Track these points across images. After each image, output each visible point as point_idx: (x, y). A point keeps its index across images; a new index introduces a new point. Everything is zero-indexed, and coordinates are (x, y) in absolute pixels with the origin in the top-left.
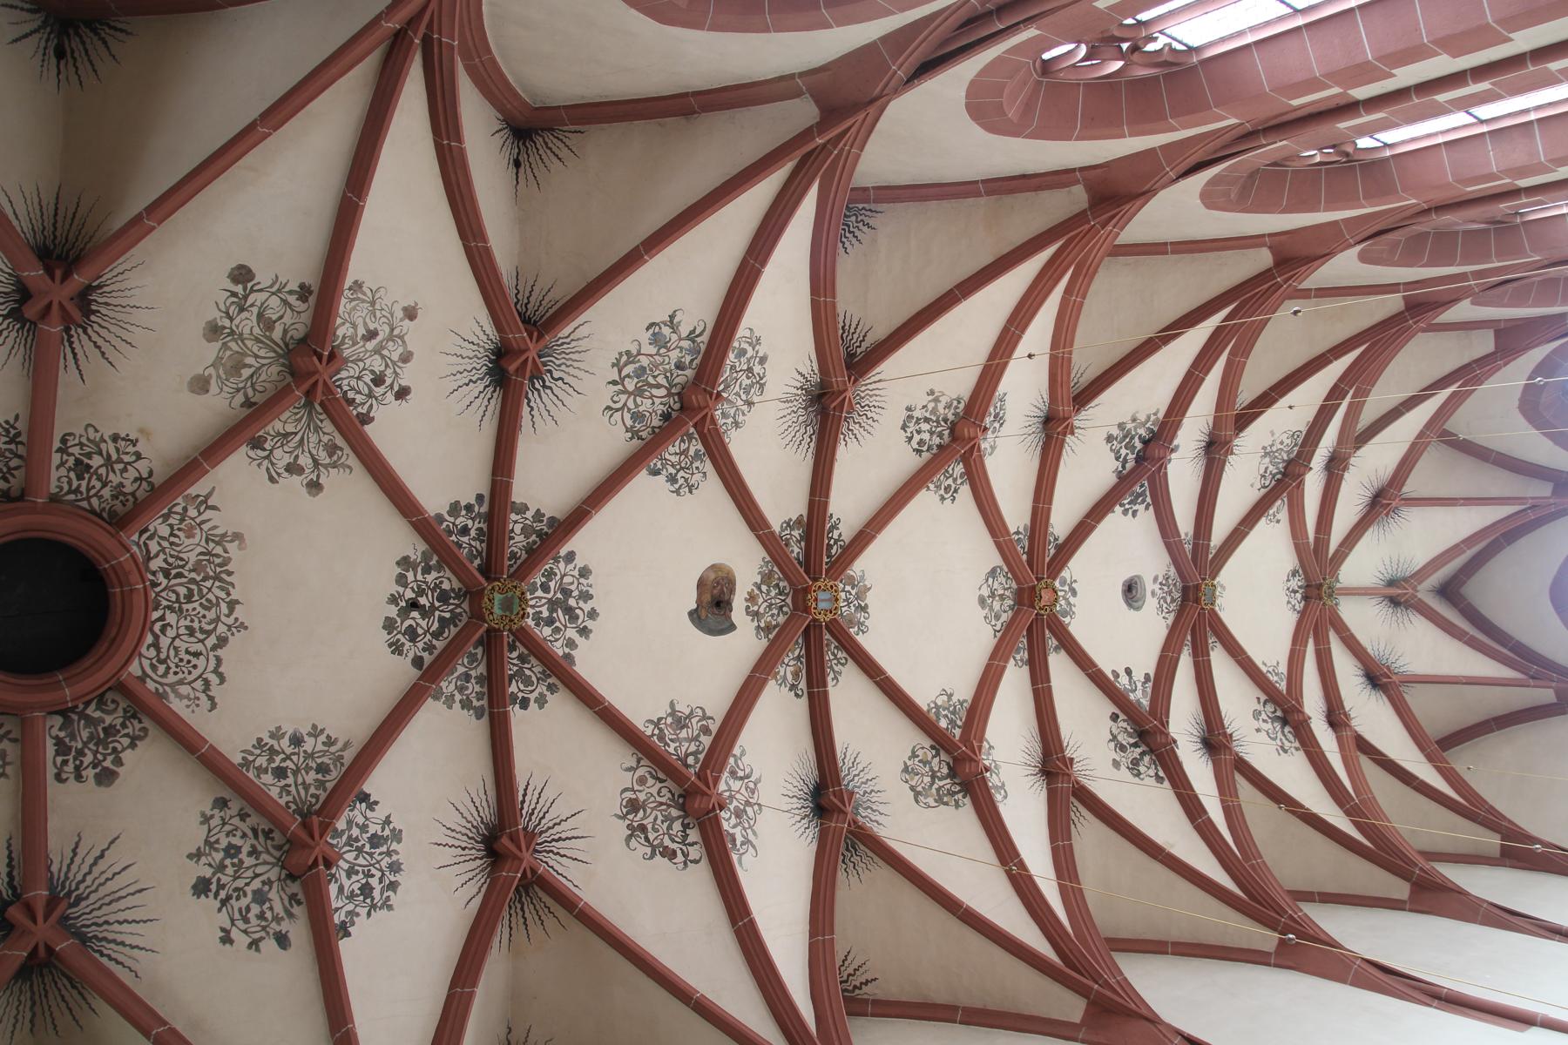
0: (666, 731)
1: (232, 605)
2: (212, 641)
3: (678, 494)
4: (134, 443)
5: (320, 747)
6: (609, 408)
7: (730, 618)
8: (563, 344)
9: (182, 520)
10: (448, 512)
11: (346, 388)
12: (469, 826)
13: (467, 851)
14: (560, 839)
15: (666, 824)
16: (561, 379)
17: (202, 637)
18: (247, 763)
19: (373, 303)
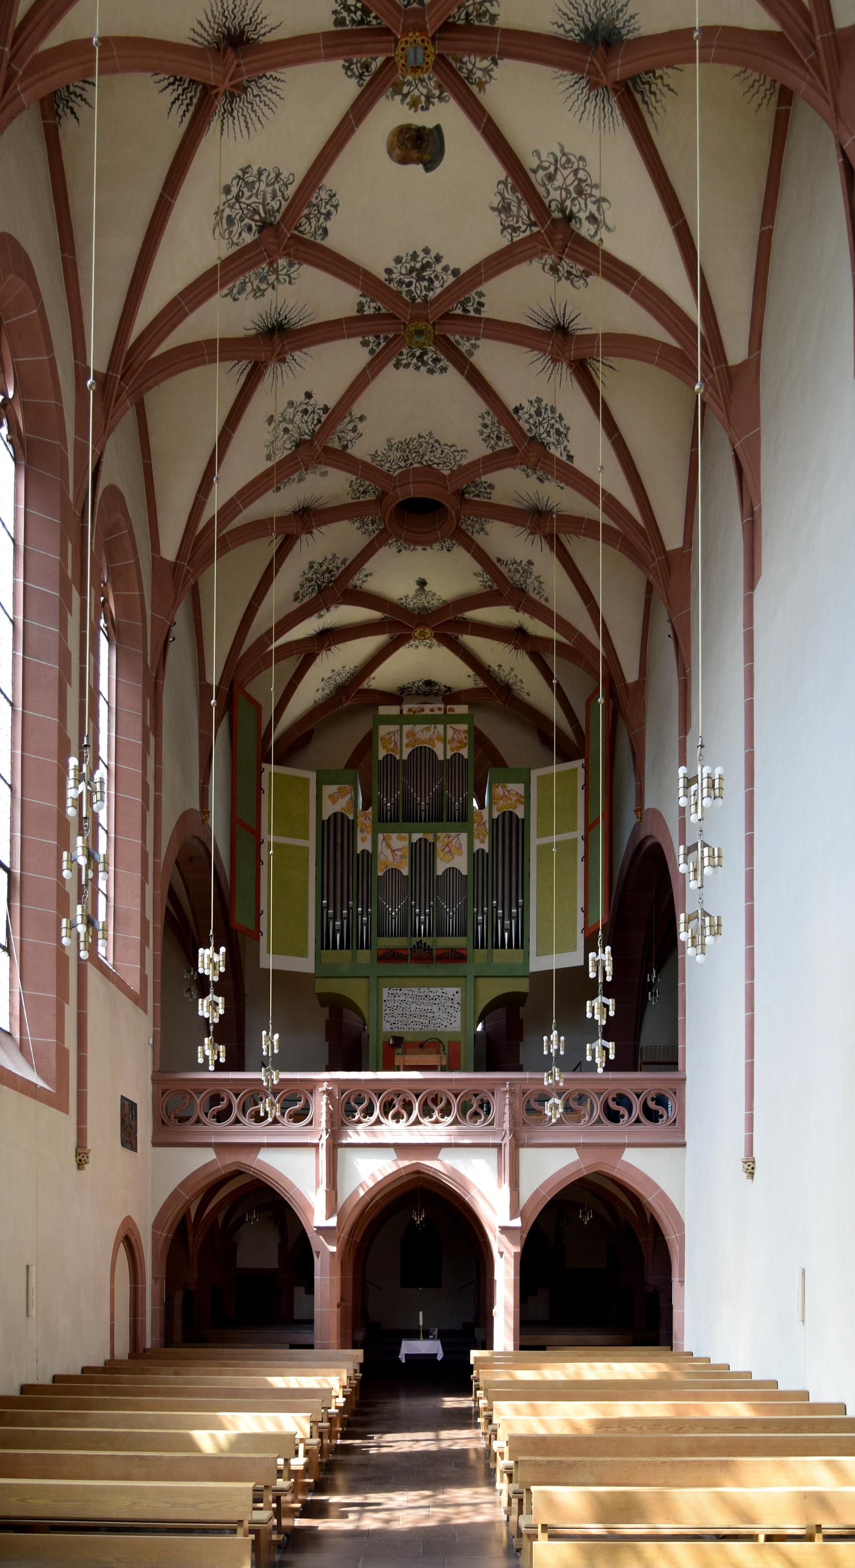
0: (511, 223)
1: (420, 436)
2: (436, 445)
7: (431, 130)
17: (434, 449)
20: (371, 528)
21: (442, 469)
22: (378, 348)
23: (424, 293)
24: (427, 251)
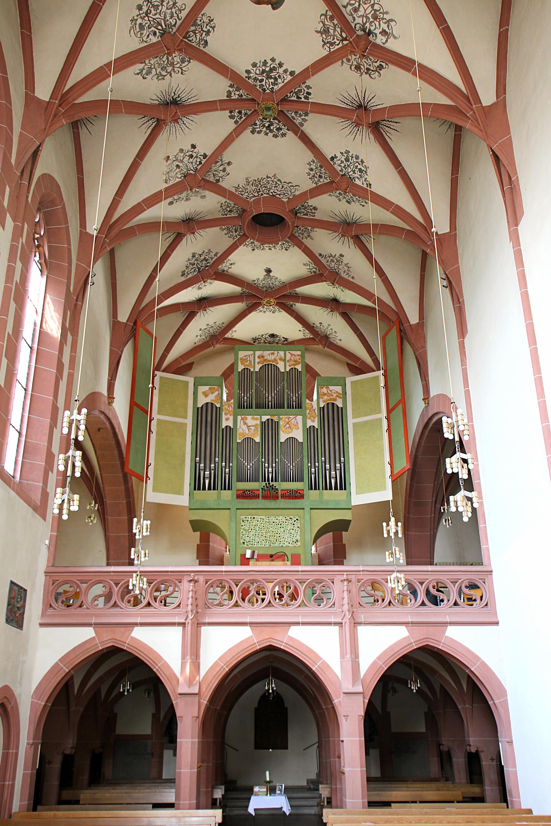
0: (329, 40)
1: (268, 177)
2: (279, 182)
3: (215, 27)
4: (222, 204)
5: (314, 164)
6: (182, 73)
8: (161, 99)
9: (243, 191)
10: (233, 119)
11: (196, 166)
12: (351, 125)
13: (359, 129)
14: (364, 98)
15: (369, 60)
16: (174, 93)
17: (277, 185)
18: (316, 183)
19: (169, 172)
20: (234, 234)
21: (282, 198)
22: (240, 120)
23: (271, 87)
24: (273, 60)
